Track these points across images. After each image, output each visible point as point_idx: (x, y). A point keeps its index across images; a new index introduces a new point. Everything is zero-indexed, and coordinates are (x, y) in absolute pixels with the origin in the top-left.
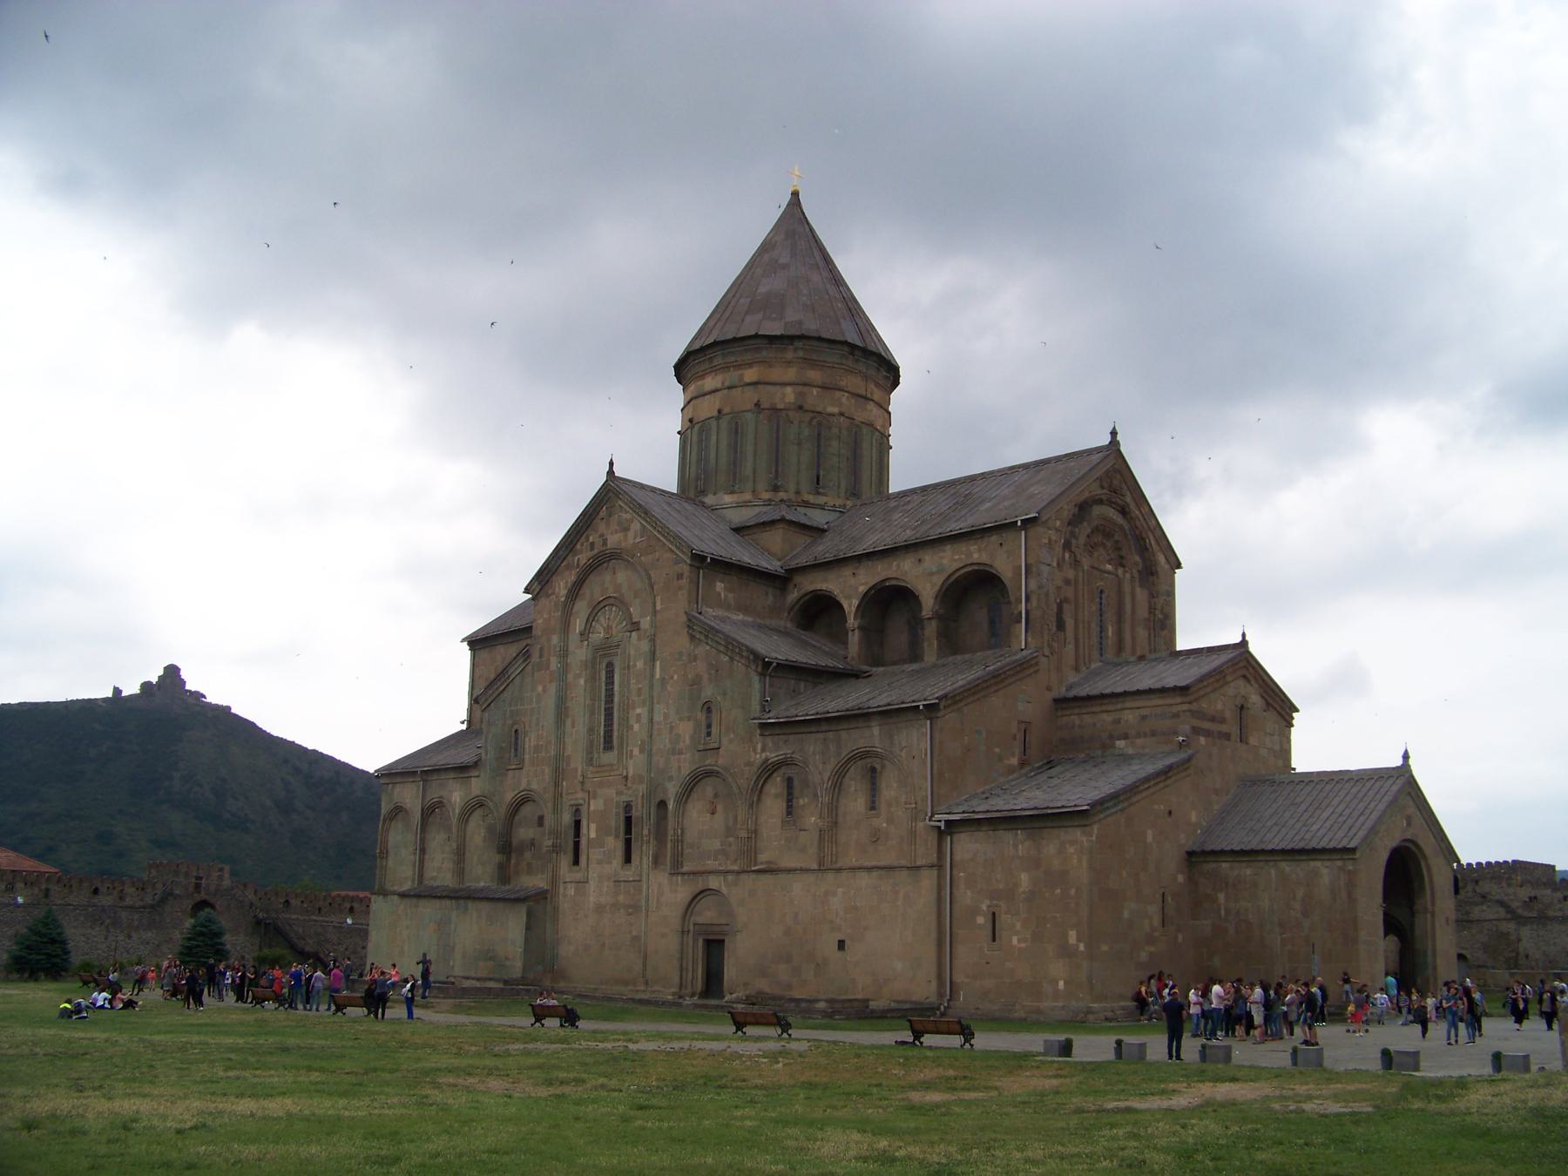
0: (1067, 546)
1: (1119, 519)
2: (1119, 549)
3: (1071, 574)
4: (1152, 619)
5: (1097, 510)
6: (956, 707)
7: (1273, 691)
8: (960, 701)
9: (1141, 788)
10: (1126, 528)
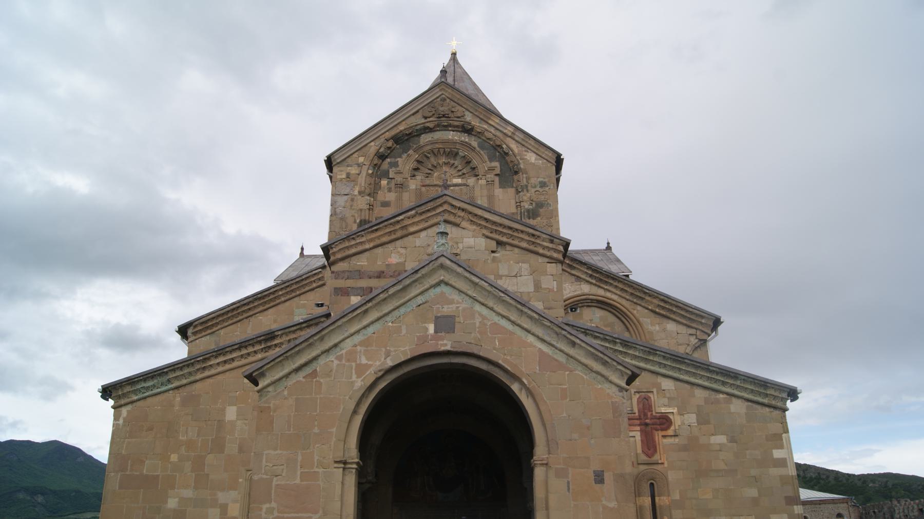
0: (378, 173)
1: (465, 138)
2: (468, 162)
3: (391, 197)
4: (519, 212)
5: (425, 139)
6: (209, 331)
7: (510, 228)
8: (217, 324)
9: (214, 361)
10: (475, 144)
